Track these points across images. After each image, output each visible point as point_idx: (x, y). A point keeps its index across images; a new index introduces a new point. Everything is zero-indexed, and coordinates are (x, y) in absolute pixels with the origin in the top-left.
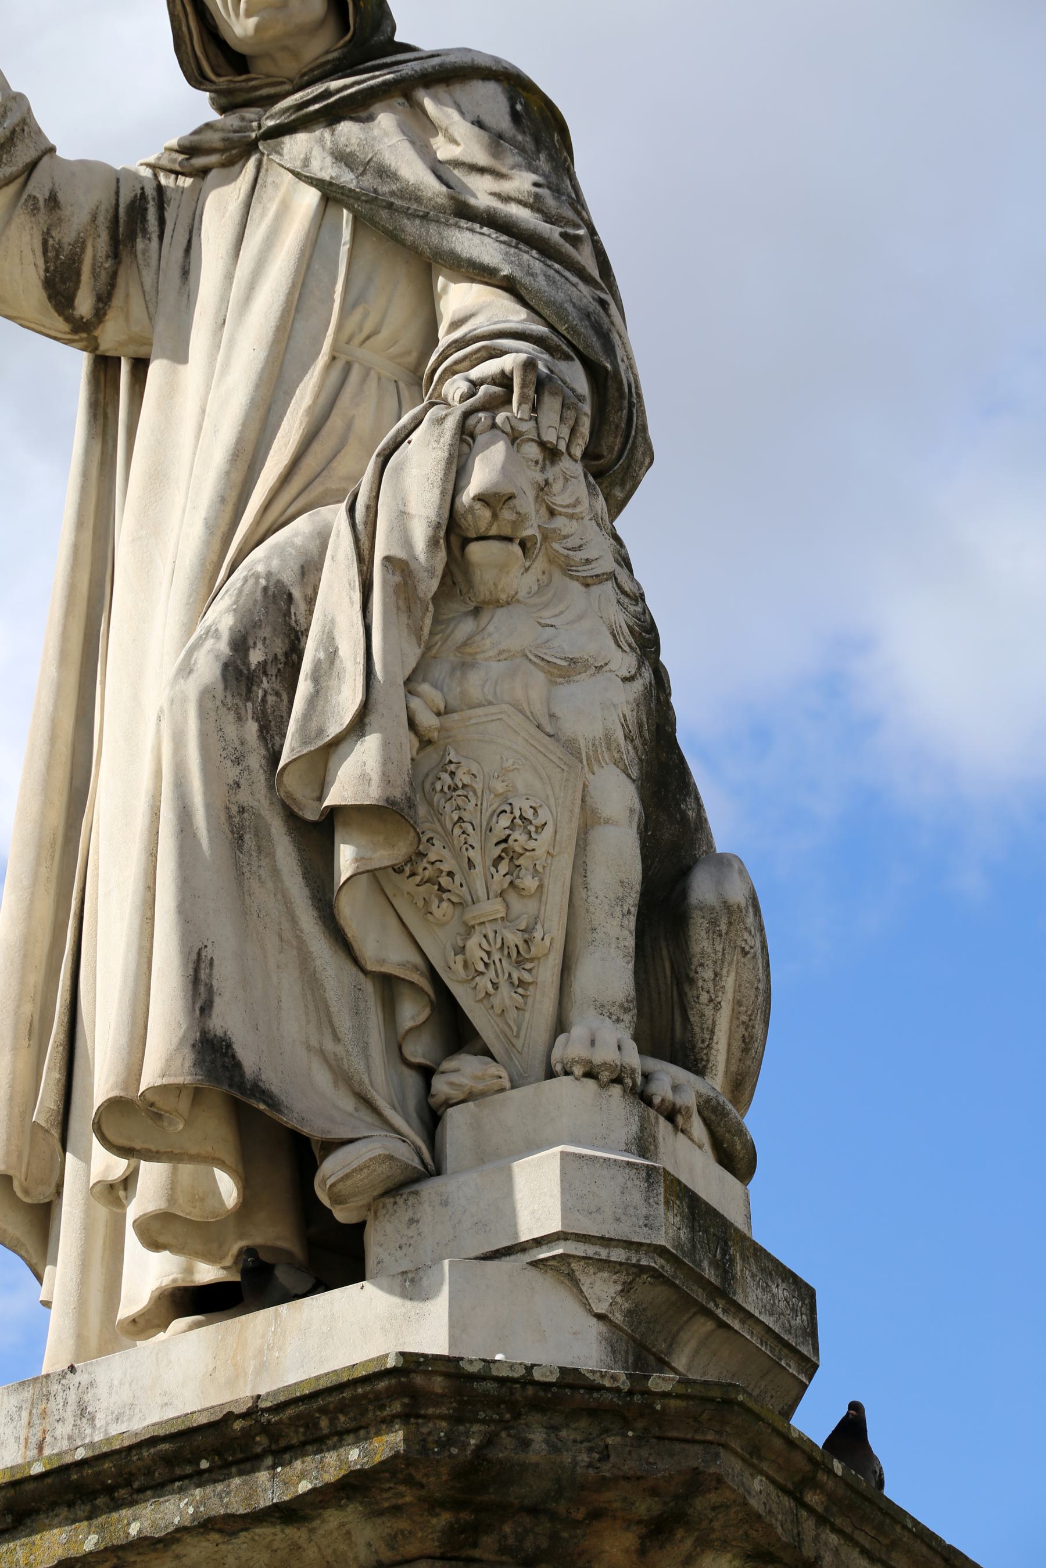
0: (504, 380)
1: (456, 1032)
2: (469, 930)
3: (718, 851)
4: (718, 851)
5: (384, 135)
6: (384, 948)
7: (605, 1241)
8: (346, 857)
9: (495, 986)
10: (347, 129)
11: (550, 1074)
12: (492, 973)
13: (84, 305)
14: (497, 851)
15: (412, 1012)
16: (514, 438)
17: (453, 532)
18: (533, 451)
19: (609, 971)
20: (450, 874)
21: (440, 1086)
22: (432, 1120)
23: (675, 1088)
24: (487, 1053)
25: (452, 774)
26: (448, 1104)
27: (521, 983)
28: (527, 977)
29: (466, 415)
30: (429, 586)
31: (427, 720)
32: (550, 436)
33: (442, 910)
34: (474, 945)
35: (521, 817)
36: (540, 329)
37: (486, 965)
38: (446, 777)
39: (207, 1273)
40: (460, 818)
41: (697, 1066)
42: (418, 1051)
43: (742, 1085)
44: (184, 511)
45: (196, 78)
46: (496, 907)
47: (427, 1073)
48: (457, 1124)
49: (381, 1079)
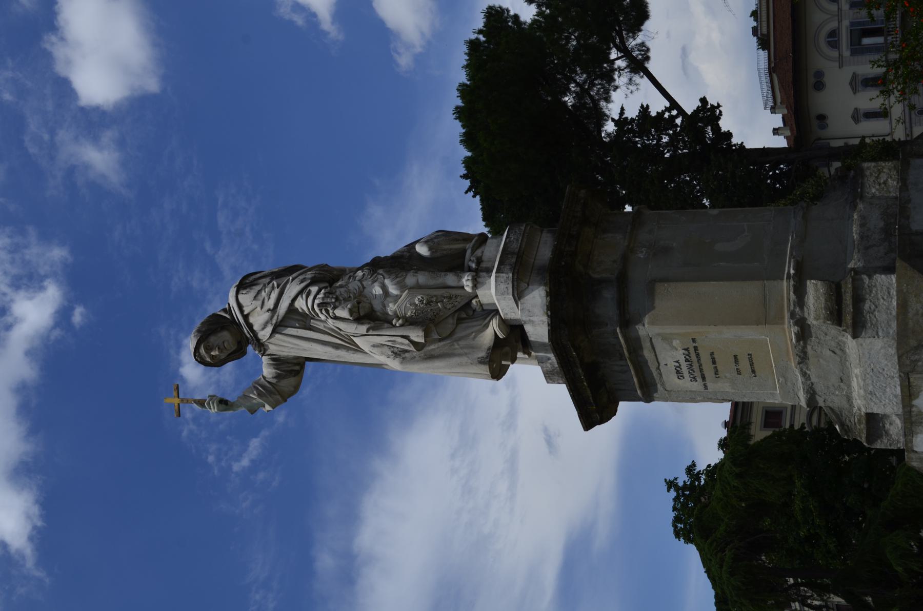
10: (255, 328)
13: (297, 368)
16: (335, 308)
18: (337, 304)
19: (450, 279)
30: (372, 324)
33: (441, 314)
34: (449, 306)
36: (304, 296)
41: (465, 251)
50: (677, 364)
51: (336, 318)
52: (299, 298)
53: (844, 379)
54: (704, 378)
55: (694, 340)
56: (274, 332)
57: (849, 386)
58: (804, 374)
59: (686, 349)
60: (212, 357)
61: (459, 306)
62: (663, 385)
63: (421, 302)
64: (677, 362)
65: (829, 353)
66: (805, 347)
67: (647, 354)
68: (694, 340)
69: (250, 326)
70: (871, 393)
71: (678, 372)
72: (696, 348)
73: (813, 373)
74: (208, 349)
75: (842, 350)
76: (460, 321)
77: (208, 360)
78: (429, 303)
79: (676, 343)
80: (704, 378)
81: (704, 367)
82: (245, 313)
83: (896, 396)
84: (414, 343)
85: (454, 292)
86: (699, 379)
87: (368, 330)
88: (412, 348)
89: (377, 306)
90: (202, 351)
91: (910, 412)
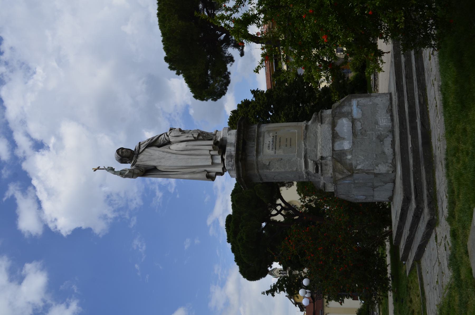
53: (316, 147)
54: (275, 149)
55: (276, 133)
56: (146, 148)
57: (317, 150)
58: (305, 144)
59: (273, 137)
62: (263, 151)
65: (313, 135)
66: (306, 133)
67: (261, 139)
68: (276, 133)
70: (323, 147)
73: (307, 144)
75: (317, 135)
77: (120, 153)
79: (271, 134)
80: (275, 149)
81: (277, 144)
83: (330, 148)
84: (194, 138)
86: (274, 149)
91: (334, 133)
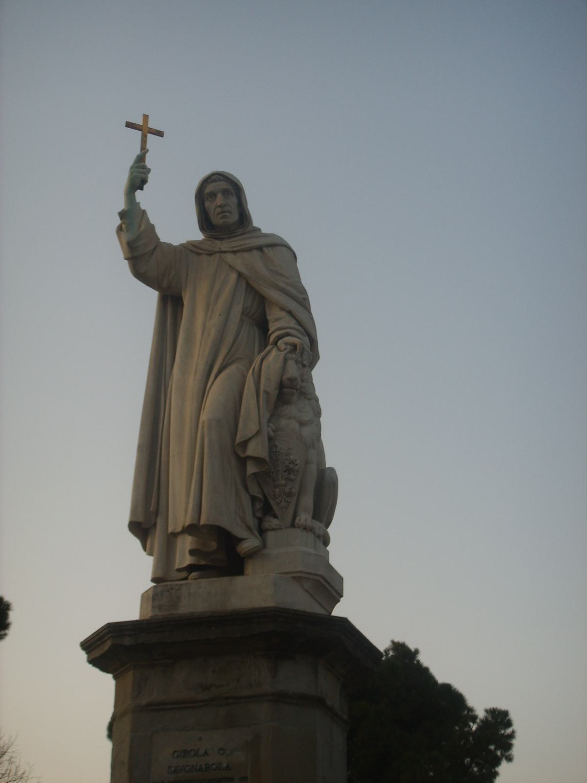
0: (294, 347)
1: (268, 510)
2: (276, 487)
3: (327, 466)
4: (327, 466)
5: (255, 258)
6: (255, 491)
7: (309, 573)
8: (251, 469)
9: (281, 502)
11: (293, 525)
12: (280, 498)
14: (285, 469)
15: (258, 506)
16: (297, 362)
17: (281, 386)
18: (300, 365)
19: (308, 501)
20: (273, 472)
21: (266, 525)
22: (262, 532)
23: (319, 528)
24: (275, 516)
25: (276, 448)
26: (267, 530)
27: (288, 502)
28: (289, 500)
29: (285, 355)
31: (272, 434)
32: (305, 363)
35: (293, 462)
37: (279, 496)
38: (274, 448)
39: (203, 563)
40: (277, 460)
41: (321, 522)
42: (259, 515)
43: (328, 524)
44: (199, 356)
45: (202, 228)
46: (283, 482)
47: (260, 520)
48: (270, 535)
49: (251, 521)
50: (201, 752)
51: (285, 360)
52: (294, 321)
59: (228, 767)
60: (213, 195)
61: (272, 503)
63: (292, 462)
64: (206, 753)
69: (249, 250)
71: (185, 753)
72: (231, 779)
74: (225, 192)
76: (254, 499)
77: (209, 188)
78: (289, 471)
82: (265, 249)
84: (245, 444)
85: (294, 500)
87: (267, 393)
88: (238, 439)
89: (290, 410)
90: (224, 185)
